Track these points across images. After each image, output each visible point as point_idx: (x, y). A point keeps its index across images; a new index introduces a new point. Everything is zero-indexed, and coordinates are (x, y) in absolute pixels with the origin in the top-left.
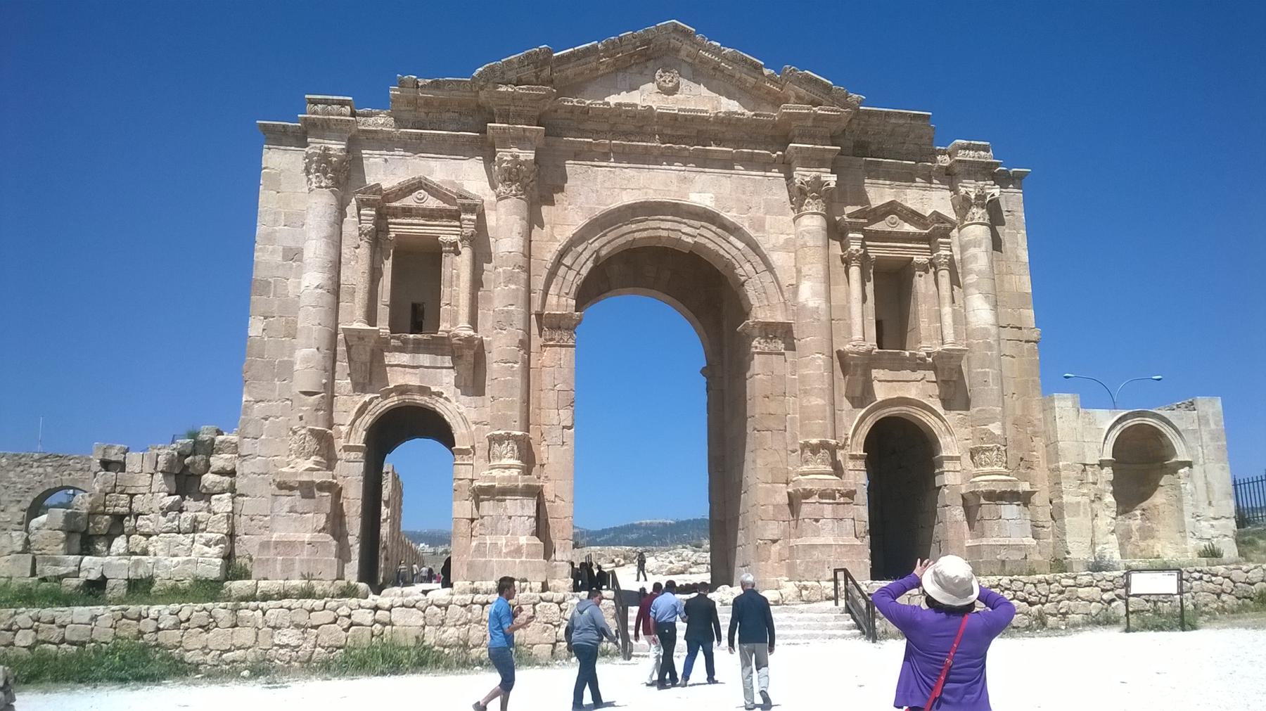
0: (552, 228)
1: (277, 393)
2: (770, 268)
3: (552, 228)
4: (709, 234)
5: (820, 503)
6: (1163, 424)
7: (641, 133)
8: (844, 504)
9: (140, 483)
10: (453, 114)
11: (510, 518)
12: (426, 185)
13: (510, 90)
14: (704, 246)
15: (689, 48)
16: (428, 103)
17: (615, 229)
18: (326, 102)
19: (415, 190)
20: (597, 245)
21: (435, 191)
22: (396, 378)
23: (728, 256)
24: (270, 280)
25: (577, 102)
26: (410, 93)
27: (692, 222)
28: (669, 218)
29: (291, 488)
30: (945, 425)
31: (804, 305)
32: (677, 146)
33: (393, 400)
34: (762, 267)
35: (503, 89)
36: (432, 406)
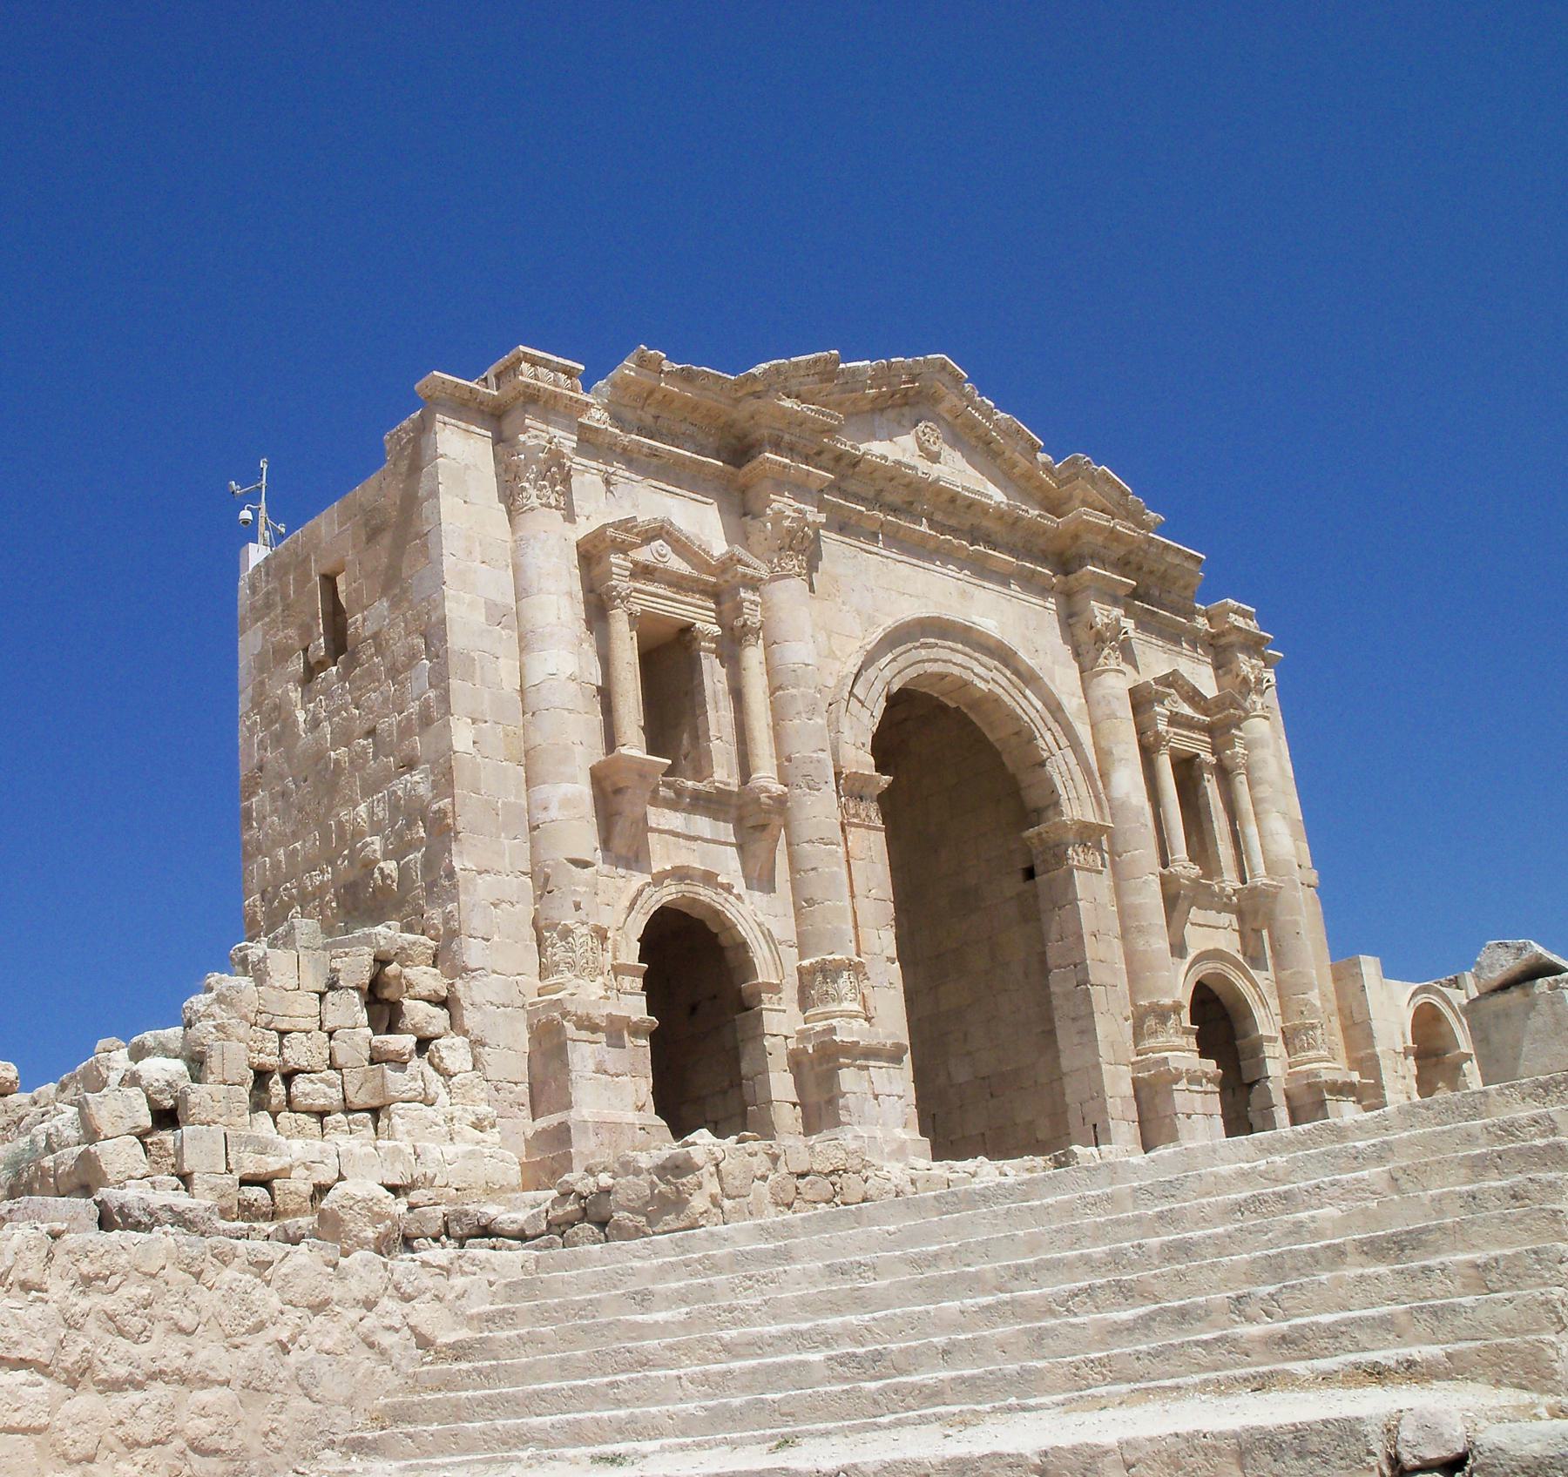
0: (829, 637)
1: (507, 860)
2: (1076, 745)
3: (829, 637)
4: (1004, 682)
5: (1190, 1091)
6: (1444, 1005)
7: (905, 509)
8: (1211, 1092)
9: (298, 1009)
10: (692, 428)
11: (876, 1097)
12: (667, 532)
13: (795, 407)
14: (997, 700)
15: (955, 400)
16: (668, 399)
17: (905, 652)
18: (547, 364)
19: (653, 539)
20: (887, 673)
21: (681, 546)
22: (663, 856)
23: (1026, 718)
24: (472, 654)
25: (851, 446)
26: (647, 380)
27: (985, 659)
28: (960, 646)
29: (594, 1028)
30: (1257, 992)
31: (1123, 802)
32: (955, 541)
33: (669, 893)
34: (1063, 742)
35: (788, 403)
36: (720, 908)
